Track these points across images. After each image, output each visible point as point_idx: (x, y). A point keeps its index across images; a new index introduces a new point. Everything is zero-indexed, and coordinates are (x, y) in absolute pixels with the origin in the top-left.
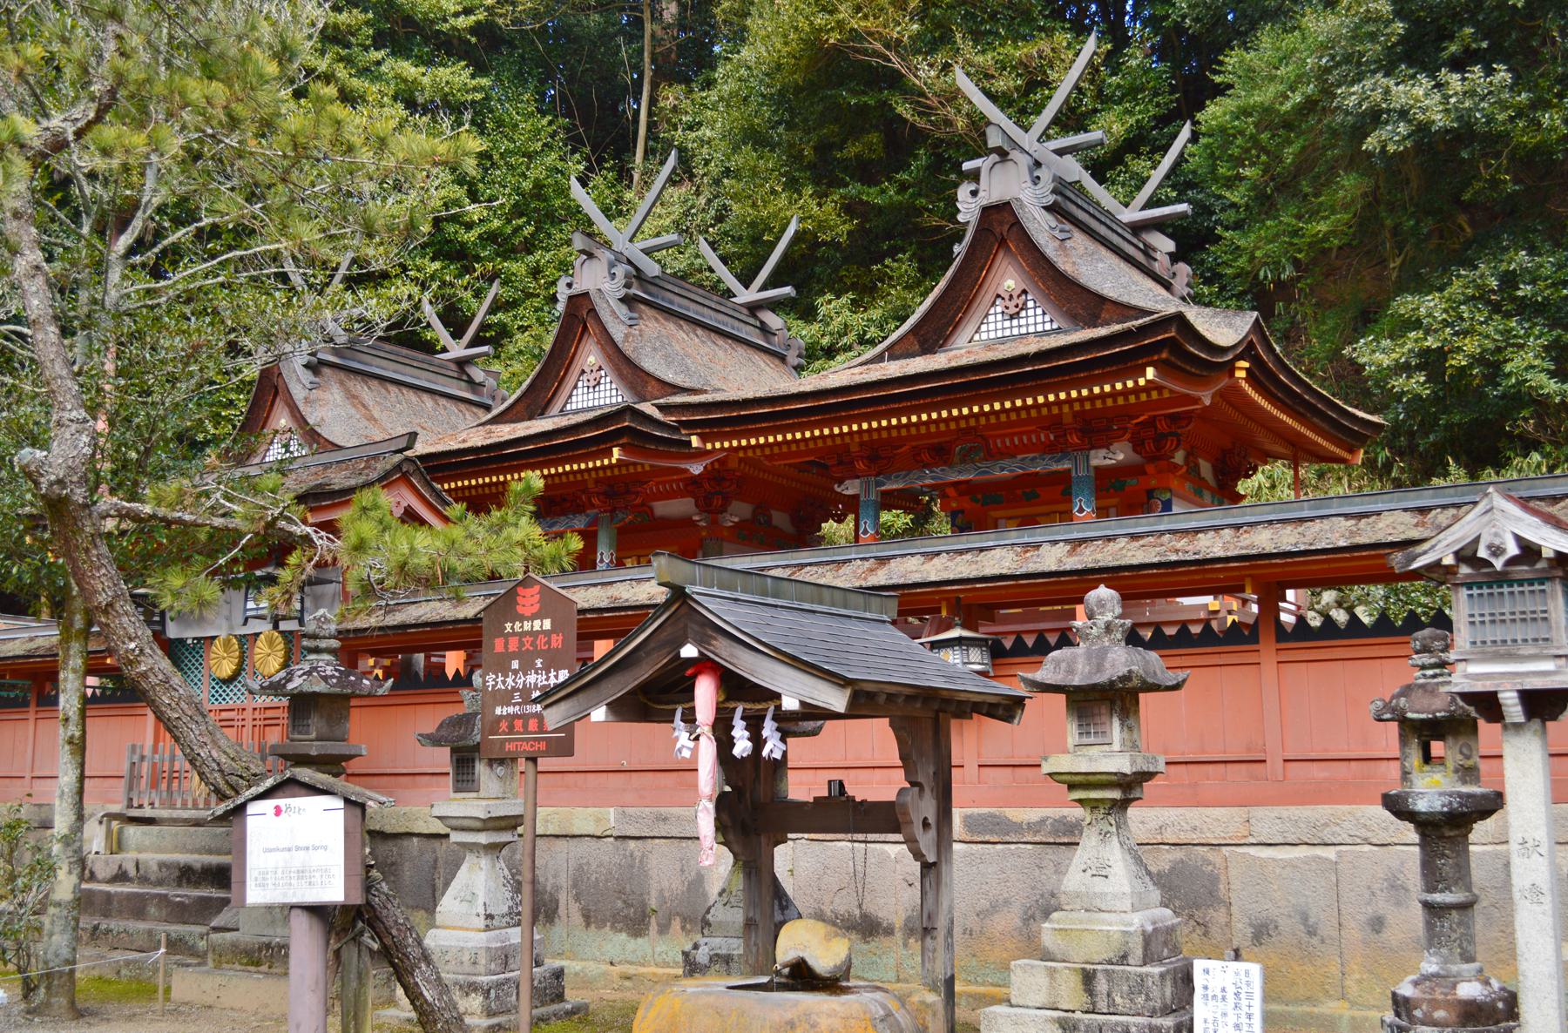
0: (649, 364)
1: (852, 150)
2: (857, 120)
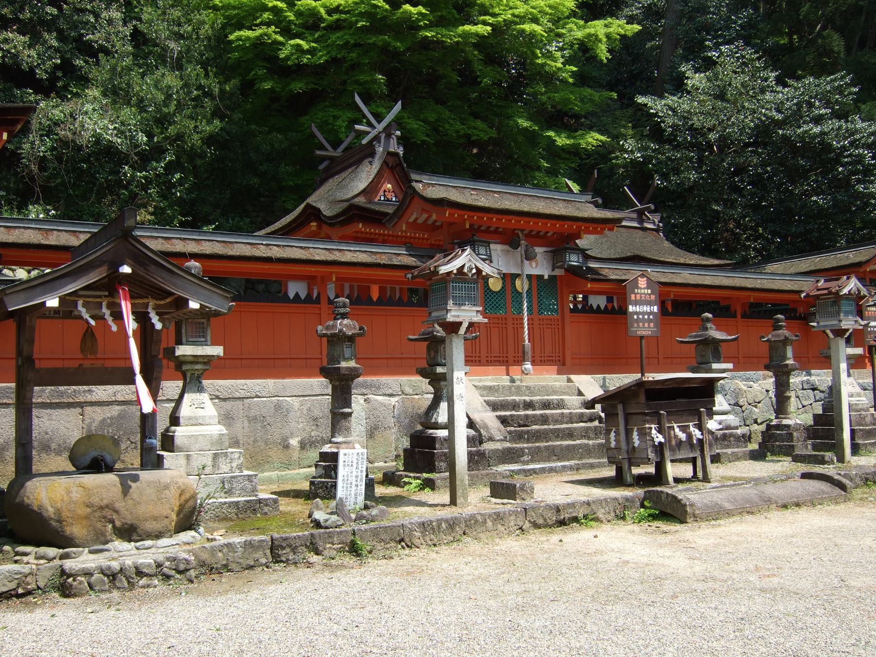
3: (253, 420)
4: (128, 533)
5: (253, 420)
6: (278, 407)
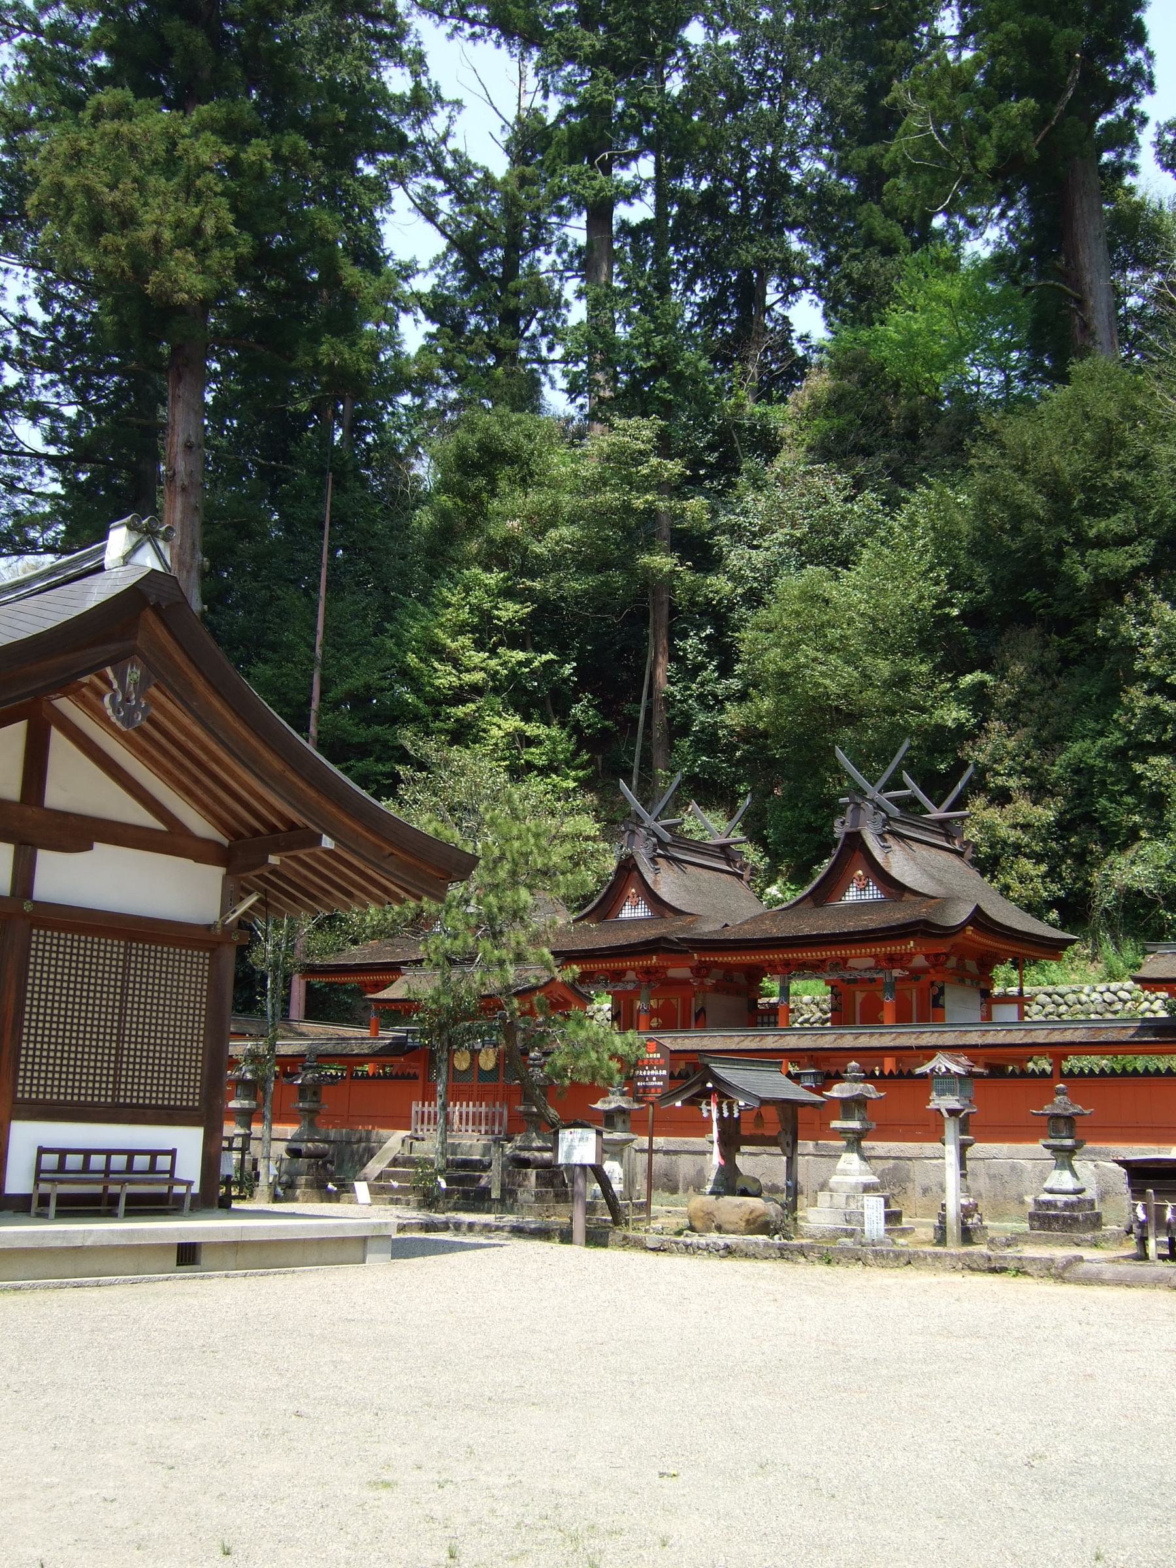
3: (992, 1177)
4: (719, 1229)
5: (992, 1177)
6: (1013, 1168)
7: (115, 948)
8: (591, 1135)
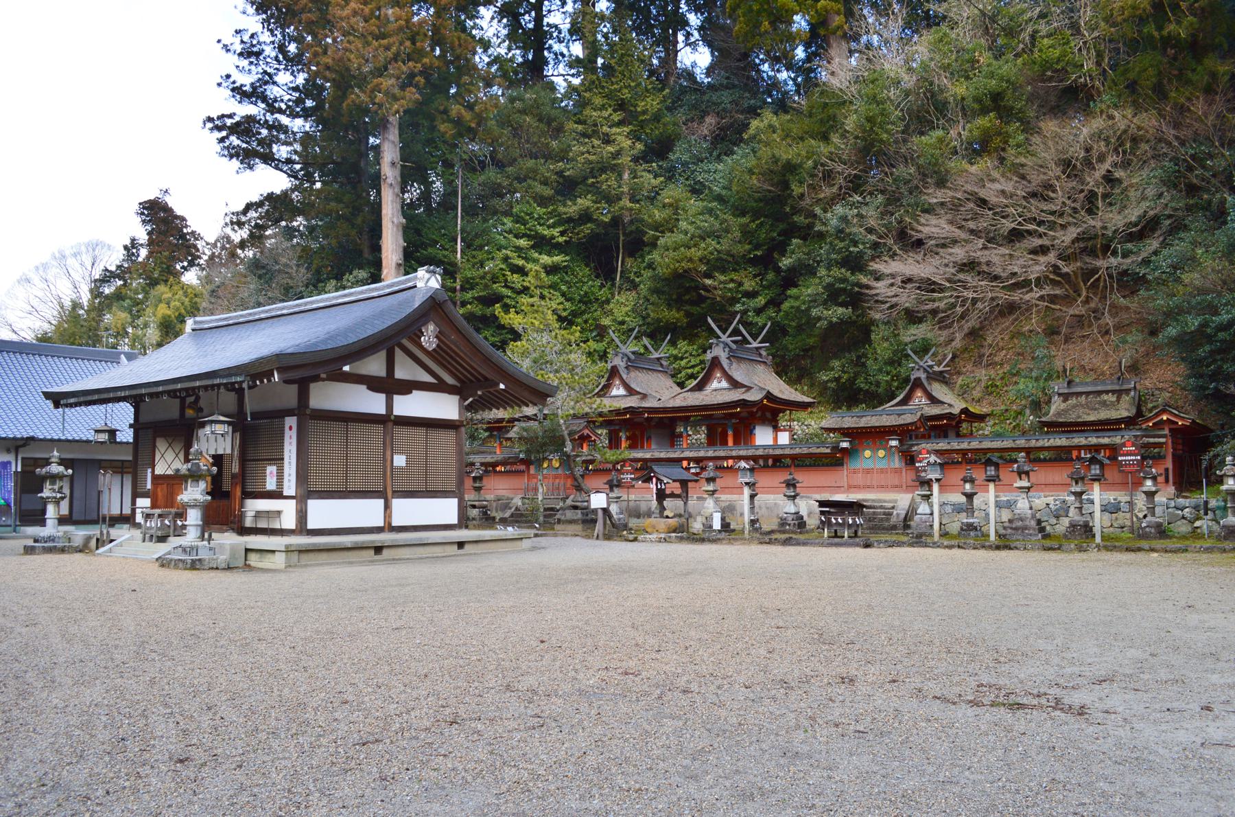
0: (633, 386)
1: (687, 297)
2: (688, 290)
7: (421, 432)
8: (604, 496)
